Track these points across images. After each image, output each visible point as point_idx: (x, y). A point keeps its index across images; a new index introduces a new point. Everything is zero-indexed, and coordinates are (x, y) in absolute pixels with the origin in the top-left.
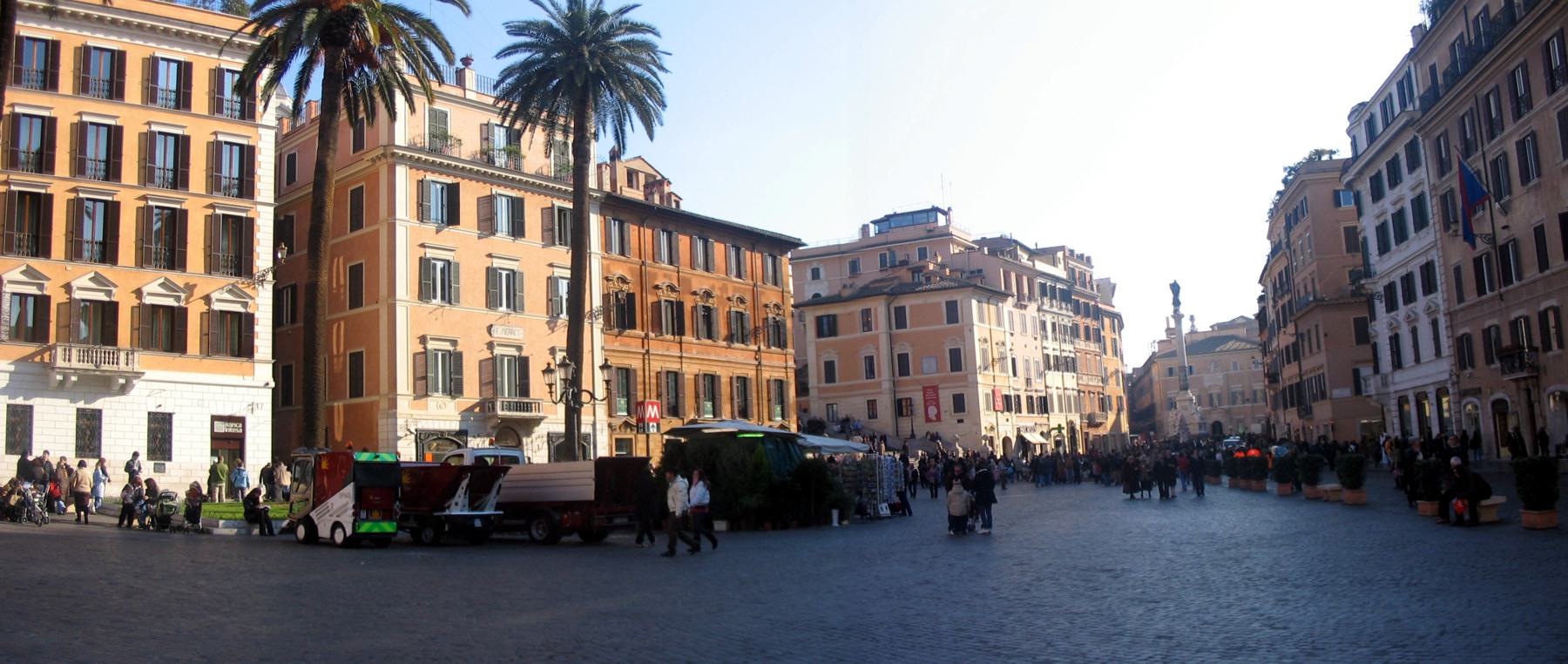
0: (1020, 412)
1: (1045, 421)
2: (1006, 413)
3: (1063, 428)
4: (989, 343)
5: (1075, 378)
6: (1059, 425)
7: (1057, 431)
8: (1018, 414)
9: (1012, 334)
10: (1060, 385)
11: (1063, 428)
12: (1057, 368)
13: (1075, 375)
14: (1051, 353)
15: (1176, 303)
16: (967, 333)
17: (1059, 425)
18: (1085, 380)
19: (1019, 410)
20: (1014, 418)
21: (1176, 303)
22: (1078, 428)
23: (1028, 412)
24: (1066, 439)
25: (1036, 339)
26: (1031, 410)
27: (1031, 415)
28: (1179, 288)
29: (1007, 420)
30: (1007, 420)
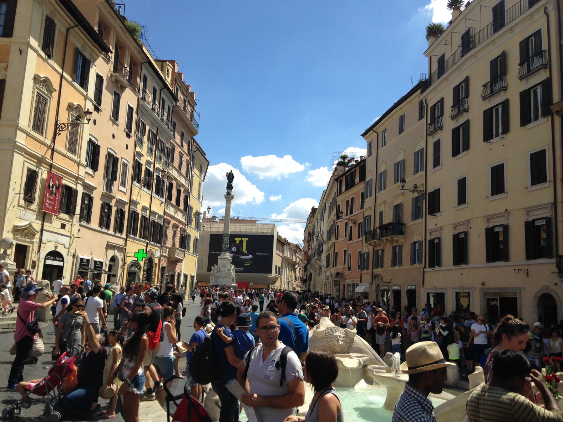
0: (88, 220)
2: (66, 216)
4: (55, 95)
5: (163, 205)
10: (148, 206)
14: (143, 161)
15: (230, 187)
16: (14, 56)
19: (86, 216)
20: (76, 227)
21: (230, 187)
22: (156, 261)
23: (101, 224)
25: (128, 136)
26: (104, 222)
27: (104, 230)
28: (233, 177)
29: (63, 226)
30: (63, 226)
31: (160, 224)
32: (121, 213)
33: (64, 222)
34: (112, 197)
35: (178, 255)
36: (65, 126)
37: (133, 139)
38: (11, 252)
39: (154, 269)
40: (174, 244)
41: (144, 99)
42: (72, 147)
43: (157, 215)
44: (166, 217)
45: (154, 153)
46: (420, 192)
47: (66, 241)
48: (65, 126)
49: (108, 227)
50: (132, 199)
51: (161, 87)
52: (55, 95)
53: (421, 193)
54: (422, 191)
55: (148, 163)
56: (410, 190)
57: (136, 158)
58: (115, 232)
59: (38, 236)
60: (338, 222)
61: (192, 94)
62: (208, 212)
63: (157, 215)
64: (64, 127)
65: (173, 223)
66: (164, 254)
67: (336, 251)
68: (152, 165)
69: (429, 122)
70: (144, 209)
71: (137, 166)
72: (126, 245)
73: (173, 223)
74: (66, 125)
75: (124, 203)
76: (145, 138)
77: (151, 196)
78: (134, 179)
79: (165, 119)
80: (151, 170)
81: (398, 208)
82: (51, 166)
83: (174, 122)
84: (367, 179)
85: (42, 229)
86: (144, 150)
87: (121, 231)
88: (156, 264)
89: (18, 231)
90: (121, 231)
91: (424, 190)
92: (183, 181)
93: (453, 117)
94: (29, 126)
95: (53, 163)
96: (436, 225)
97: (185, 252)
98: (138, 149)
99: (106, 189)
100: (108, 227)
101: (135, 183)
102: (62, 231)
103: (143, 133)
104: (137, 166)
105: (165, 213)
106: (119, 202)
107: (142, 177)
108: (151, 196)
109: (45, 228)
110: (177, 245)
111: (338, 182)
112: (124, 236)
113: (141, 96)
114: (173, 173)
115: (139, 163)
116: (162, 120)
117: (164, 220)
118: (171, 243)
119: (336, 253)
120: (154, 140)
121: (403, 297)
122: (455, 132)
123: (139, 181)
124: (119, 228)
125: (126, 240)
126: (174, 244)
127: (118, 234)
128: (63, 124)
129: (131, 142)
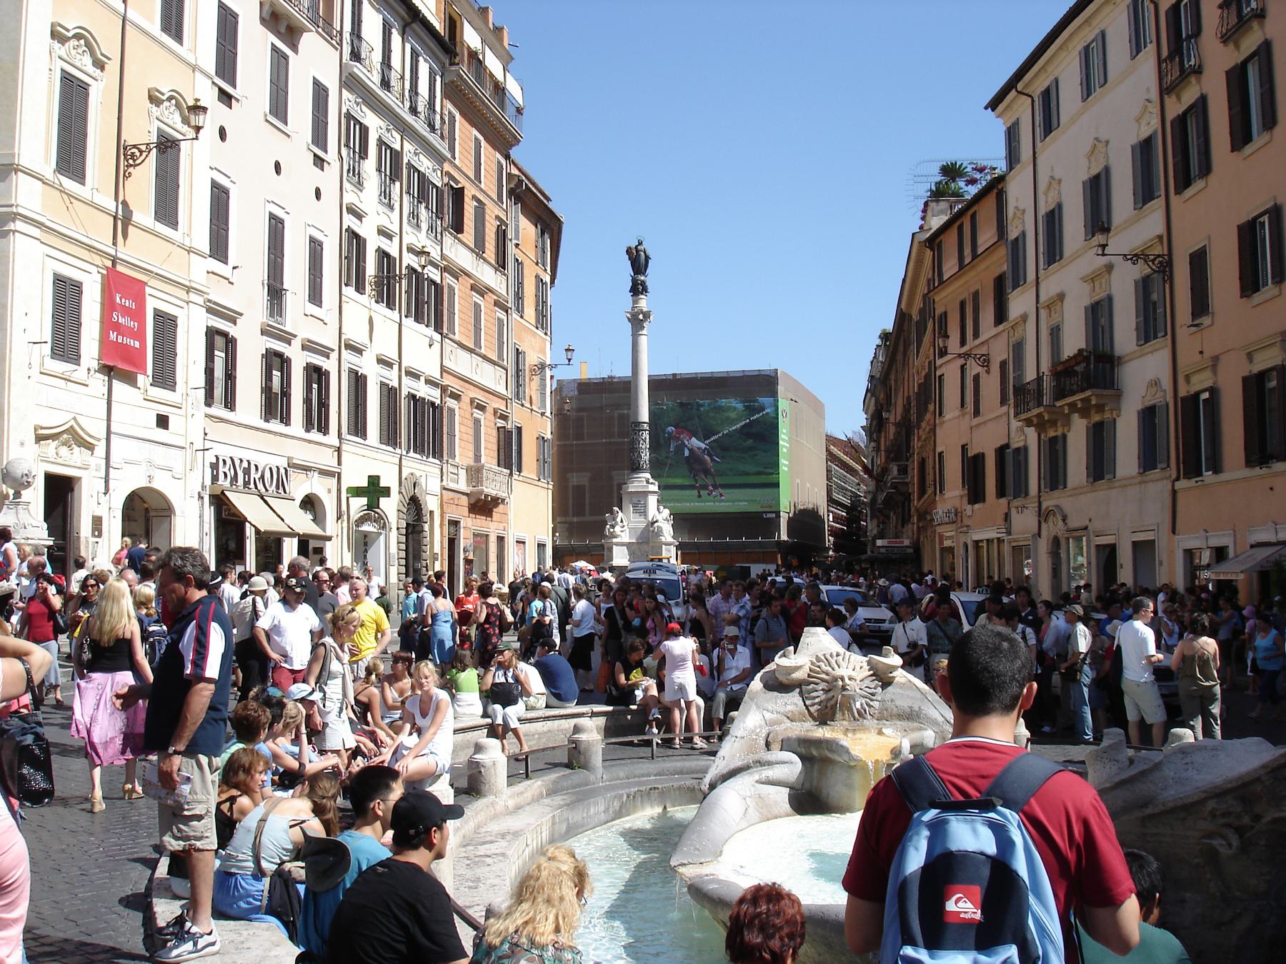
1: (328, 460)
3: (386, 492)
5: (437, 346)
6: (374, 480)
7: (364, 501)
8: (218, 410)
9: (226, 98)
11: (386, 492)
12: (385, 294)
13: (437, 337)
14: (366, 230)
17: (374, 480)
18: (463, 363)
21: (638, 289)
22: (431, 504)
24: (394, 535)
25: (319, 162)
26: (275, 405)
28: (647, 258)
29: (163, 422)
30: (163, 422)
31: (433, 404)
32: (316, 375)
33: (164, 410)
34: (287, 338)
35: (490, 488)
36: (141, 152)
37: (333, 170)
38: (35, 496)
39: (426, 527)
40: (477, 457)
41: (356, 56)
42: (167, 210)
43: (422, 379)
44: (448, 381)
45: (397, 206)
46: (1153, 261)
47: (175, 459)
48: (141, 152)
49: (286, 420)
50: (344, 337)
51: (403, 19)
52: (112, 67)
53: (1156, 262)
54: (1159, 256)
55: (382, 232)
56: (1125, 255)
57: (349, 221)
58: (308, 430)
59: (100, 449)
60: (941, 366)
61: (498, 30)
62: (569, 360)
63: (422, 379)
64: (138, 154)
65: (471, 398)
66: (452, 486)
67: (939, 450)
68: (396, 240)
69: (1165, 53)
70: (382, 361)
71: (355, 241)
72: (339, 463)
73: (471, 398)
74: (143, 148)
75: (325, 352)
76: (369, 165)
77: (400, 325)
78: (344, 281)
79: (420, 108)
80: (394, 252)
81: (1099, 314)
82: (114, 261)
83: (450, 113)
84: (1013, 234)
85: (109, 432)
86: (369, 198)
87: (324, 429)
88: (431, 512)
89: (46, 438)
90: (324, 429)
91: (1166, 252)
92: (488, 276)
93: (1226, 34)
94: (47, 160)
95: (119, 255)
96: (1201, 352)
97: (511, 474)
98: (350, 198)
99: (272, 315)
100: (286, 420)
101: (350, 291)
102: (160, 434)
103: (363, 154)
104: (355, 241)
105: (443, 370)
106: (308, 346)
107: (368, 274)
108: (400, 325)
109: (113, 429)
110: (489, 458)
111: (932, 250)
112: (332, 439)
113: (347, 49)
114: (456, 257)
115: (356, 236)
116: (414, 111)
117: (444, 389)
118: (471, 455)
119: (941, 454)
120: (393, 166)
121: (1121, 567)
122: (1237, 78)
123: (360, 288)
124: (317, 419)
125: (339, 450)
126: (477, 457)
127: (315, 435)
128: (135, 146)
129: (329, 178)
